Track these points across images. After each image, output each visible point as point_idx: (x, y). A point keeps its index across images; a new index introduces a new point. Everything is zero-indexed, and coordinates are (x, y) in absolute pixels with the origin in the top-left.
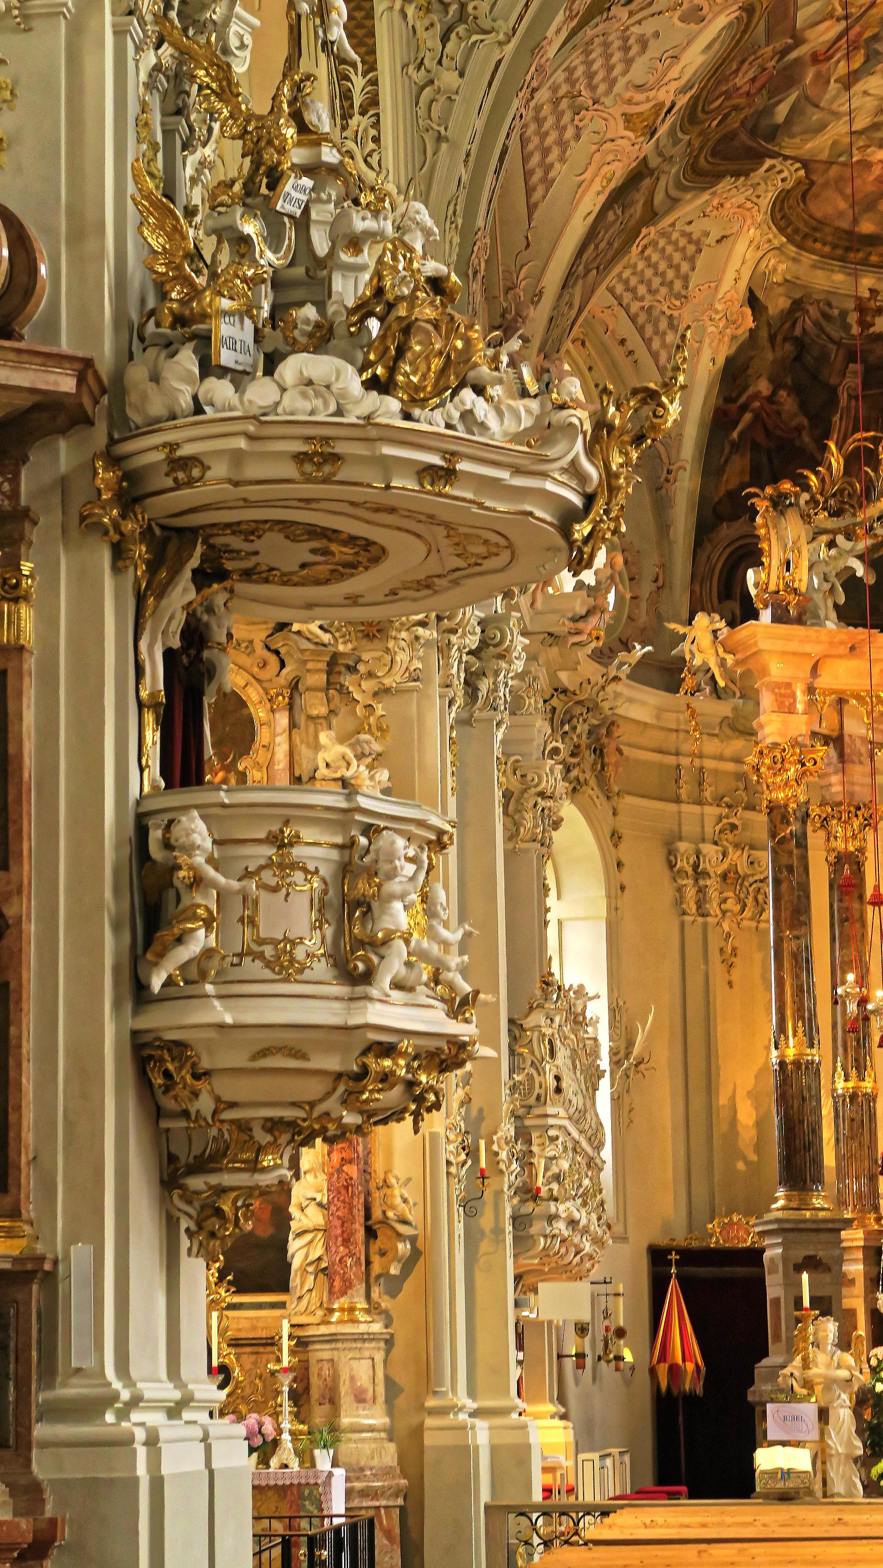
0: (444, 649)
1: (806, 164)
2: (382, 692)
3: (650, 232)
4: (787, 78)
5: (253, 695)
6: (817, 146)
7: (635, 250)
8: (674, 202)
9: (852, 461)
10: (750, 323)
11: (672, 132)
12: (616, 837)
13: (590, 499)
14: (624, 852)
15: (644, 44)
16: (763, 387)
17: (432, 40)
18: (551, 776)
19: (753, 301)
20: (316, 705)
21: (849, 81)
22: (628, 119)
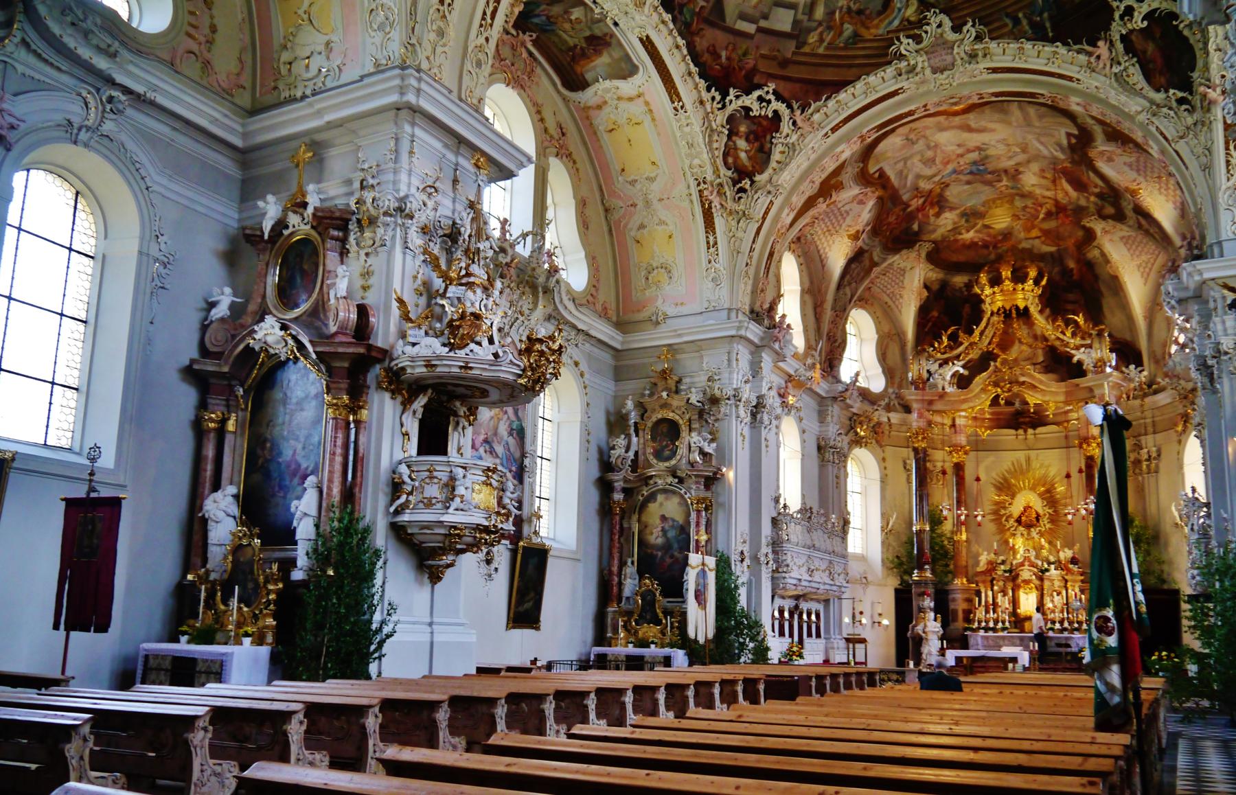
0: (737, 406)
1: (934, 242)
2: (717, 420)
3: (876, 270)
4: (911, 217)
5: (681, 422)
6: (937, 235)
7: (873, 275)
8: (885, 260)
9: (949, 338)
10: (926, 294)
11: (869, 238)
12: (884, 459)
13: (524, 370)
14: (888, 464)
15: (848, 213)
16: (935, 314)
17: (734, 223)
18: (843, 442)
19: (926, 286)
20: (695, 425)
21: (938, 215)
22: (849, 237)
